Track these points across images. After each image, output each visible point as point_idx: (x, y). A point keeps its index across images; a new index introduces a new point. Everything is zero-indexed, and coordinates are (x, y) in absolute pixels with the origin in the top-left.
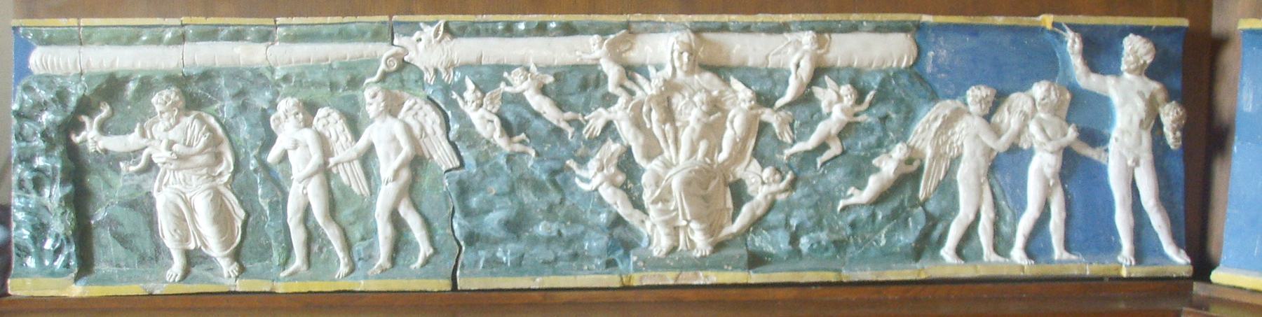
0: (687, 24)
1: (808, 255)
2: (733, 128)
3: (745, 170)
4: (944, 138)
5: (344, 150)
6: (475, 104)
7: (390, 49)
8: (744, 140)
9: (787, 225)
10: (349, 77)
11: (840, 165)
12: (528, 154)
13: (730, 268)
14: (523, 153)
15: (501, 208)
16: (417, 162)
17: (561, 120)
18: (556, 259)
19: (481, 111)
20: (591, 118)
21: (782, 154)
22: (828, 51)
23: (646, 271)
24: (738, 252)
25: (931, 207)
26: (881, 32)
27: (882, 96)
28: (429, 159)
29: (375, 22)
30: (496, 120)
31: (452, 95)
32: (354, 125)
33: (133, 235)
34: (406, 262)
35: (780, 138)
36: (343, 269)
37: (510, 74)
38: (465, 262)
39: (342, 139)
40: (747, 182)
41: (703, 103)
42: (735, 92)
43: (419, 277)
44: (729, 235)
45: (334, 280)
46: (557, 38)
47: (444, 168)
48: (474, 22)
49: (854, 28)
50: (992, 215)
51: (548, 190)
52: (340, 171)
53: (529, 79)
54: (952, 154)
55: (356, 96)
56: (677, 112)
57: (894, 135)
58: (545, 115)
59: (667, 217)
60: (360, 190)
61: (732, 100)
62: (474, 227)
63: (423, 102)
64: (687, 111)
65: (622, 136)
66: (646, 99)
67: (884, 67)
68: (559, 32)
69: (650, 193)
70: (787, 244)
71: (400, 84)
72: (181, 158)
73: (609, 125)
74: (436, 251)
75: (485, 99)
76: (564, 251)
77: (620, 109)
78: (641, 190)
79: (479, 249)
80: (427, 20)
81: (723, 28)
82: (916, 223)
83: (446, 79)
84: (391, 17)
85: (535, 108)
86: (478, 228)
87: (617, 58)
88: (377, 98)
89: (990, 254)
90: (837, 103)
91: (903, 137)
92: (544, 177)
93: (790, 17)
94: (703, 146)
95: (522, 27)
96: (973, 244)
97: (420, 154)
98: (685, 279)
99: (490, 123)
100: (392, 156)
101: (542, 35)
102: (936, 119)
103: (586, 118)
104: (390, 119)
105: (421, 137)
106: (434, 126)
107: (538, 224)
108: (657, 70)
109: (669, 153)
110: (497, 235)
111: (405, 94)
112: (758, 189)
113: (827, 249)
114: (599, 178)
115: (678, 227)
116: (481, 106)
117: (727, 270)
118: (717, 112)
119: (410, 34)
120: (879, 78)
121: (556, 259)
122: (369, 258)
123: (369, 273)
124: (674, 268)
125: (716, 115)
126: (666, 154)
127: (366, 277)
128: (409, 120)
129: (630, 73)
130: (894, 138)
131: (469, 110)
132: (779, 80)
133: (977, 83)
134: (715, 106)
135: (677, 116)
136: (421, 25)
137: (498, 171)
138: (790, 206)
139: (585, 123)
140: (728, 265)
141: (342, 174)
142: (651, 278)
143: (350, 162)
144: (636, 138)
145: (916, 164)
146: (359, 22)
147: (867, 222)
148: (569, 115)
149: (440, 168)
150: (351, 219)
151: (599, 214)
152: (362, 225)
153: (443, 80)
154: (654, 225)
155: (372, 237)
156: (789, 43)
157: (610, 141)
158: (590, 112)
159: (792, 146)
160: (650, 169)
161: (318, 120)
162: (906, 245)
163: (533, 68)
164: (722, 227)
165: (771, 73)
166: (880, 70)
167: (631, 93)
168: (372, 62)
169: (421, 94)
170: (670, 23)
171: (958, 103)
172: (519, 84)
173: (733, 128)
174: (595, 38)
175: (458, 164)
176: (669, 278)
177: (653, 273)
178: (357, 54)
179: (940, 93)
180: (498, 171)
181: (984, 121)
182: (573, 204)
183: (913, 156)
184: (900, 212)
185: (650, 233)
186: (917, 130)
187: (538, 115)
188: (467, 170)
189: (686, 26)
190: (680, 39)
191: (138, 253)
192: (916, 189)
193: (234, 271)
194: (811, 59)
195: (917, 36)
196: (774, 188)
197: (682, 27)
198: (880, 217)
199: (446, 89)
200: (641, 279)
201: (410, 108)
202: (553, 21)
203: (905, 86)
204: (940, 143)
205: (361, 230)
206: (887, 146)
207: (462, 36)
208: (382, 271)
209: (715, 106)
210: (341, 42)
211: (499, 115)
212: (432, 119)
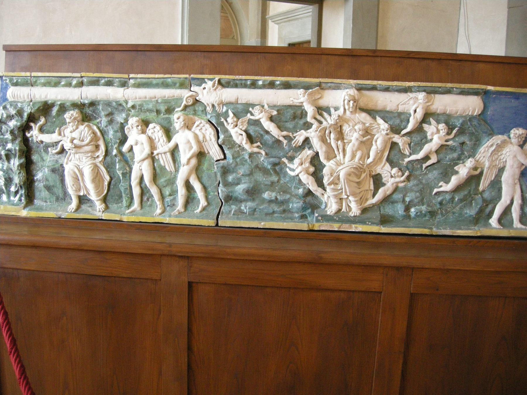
0: (353, 85)
1: (414, 218)
2: (376, 145)
3: (382, 169)
4: (496, 156)
5: (162, 147)
6: (232, 125)
7: (188, 93)
8: (383, 151)
9: (404, 201)
10: (166, 107)
11: (435, 169)
12: (261, 154)
13: (370, 223)
14: (259, 153)
15: (245, 183)
16: (201, 155)
17: (280, 136)
18: (274, 212)
19: (236, 128)
20: (297, 136)
21: (403, 161)
22: (432, 104)
23: (322, 222)
24: (375, 215)
25: (486, 195)
26: (463, 94)
27: (462, 132)
28: (207, 154)
29: (181, 78)
30: (244, 134)
31: (221, 119)
32: (168, 133)
33: (53, 186)
34: (192, 209)
35: (402, 152)
36: (159, 211)
37: (253, 109)
38: (224, 211)
39: (161, 141)
40: (383, 175)
41: (360, 130)
42: (378, 124)
43: (197, 218)
44: (370, 205)
45: (153, 216)
46: (280, 90)
47: (215, 159)
48: (234, 80)
49: (448, 92)
50: (520, 202)
51: (271, 174)
52: (160, 158)
53: (263, 112)
54: (499, 166)
55: (170, 118)
56: (345, 134)
57: (467, 153)
58: (271, 133)
59: (336, 193)
60: (170, 169)
61: (377, 129)
62: (229, 192)
63: (205, 122)
64: (351, 134)
65: (313, 146)
66: (328, 126)
67: (464, 115)
68: (281, 86)
69: (327, 179)
70: (403, 212)
71: (194, 112)
72: (76, 147)
73: (307, 140)
74: (209, 204)
75: (238, 122)
76: (278, 208)
77: (313, 131)
78: (322, 177)
79: (231, 205)
80: (209, 77)
81: (374, 88)
82: (477, 204)
83: (218, 110)
84: (190, 75)
85: (266, 128)
86: (231, 193)
87: (314, 102)
88: (180, 119)
89: (517, 223)
90: (436, 134)
91: (472, 155)
92: (269, 167)
93: (412, 84)
94: (359, 154)
95: (260, 83)
96: (508, 217)
97: (202, 151)
98: (344, 228)
99: (241, 136)
100: (187, 151)
101: (272, 88)
102: (492, 145)
103: (294, 135)
104: (187, 131)
105: (204, 141)
106: (210, 136)
107: (264, 193)
108: (335, 111)
109: (340, 157)
110: (242, 198)
111: (196, 118)
112: (388, 180)
113: (425, 216)
114: (300, 168)
115: (342, 199)
116: (236, 126)
117: (368, 224)
118: (367, 136)
119: (200, 85)
120: (461, 121)
121: (274, 212)
122: (173, 205)
123: (172, 214)
124: (338, 221)
125: (367, 137)
126: (338, 158)
127: (170, 216)
128: (197, 132)
129: (320, 111)
130: (467, 155)
131: (229, 127)
132: (404, 119)
133: (517, 126)
134: (367, 132)
135: (345, 137)
136: (206, 80)
137: (244, 162)
138: (405, 191)
139: (293, 138)
140: (369, 222)
141: (161, 160)
142: (325, 226)
143: (165, 153)
144: (321, 148)
145: (479, 170)
146: (173, 78)
147: (449, 202)
148: (285, 133)
149: (213, 159)
150: (165, 184)
151: (299, 189)
152: (170, 187)
153: (217, 111)
154: (329, 197)
155: (175, 195)
156: (412, 98)
157: (307, 149)
158: (297, 132)
159: (409, 157)
160: (329, 166)
161: (149, 130)
162: (471, 216)
163: (266, 107)
164: (367, 200)
165: (400, 114)
166: (461, 116)
167: (320, 123)
168: (179, 100)
169: (205, 118)
170: (344, 84)
171: (505, 137)
172: (257, 114)
173: (376, 145)
174: (302, 91)
175: (223, 157)
176: (335, 227)
177: (326, 224)
178: (171, 95)
179: (496, 131)
180: (244, 162)
181: (519, 148)
182: (285, 182)
183: (478, 166)
184: (468, 197)
185: (326, 201)
186: (481, 151)
187: (267, 132)
188: (228, 161)
189: (352, 86)
190: (348, 93)
191: (55, 195)
192: (478, 184)
193: (102, 208)
194: (423, 108)
195: (484, 97)
196: (398, 180)
197: (350, 87)
198: (456, 199)
199: (218, 116)
200: (320, 226)
201: (198, 126)
202: (279, 80)
203: (475, 126)
204: (494, 159)
205: (170, 190)
206: (463, 160)
207: (228, 87)
208: (179, 213)
209: (367, 132)
210: (163, 89)
211: (246, 131)
212: (210, 132)
